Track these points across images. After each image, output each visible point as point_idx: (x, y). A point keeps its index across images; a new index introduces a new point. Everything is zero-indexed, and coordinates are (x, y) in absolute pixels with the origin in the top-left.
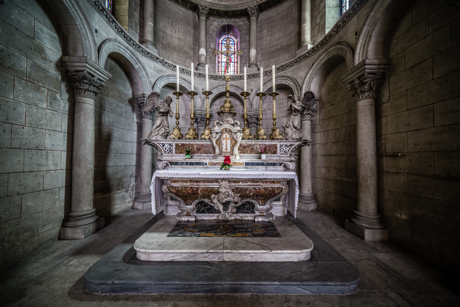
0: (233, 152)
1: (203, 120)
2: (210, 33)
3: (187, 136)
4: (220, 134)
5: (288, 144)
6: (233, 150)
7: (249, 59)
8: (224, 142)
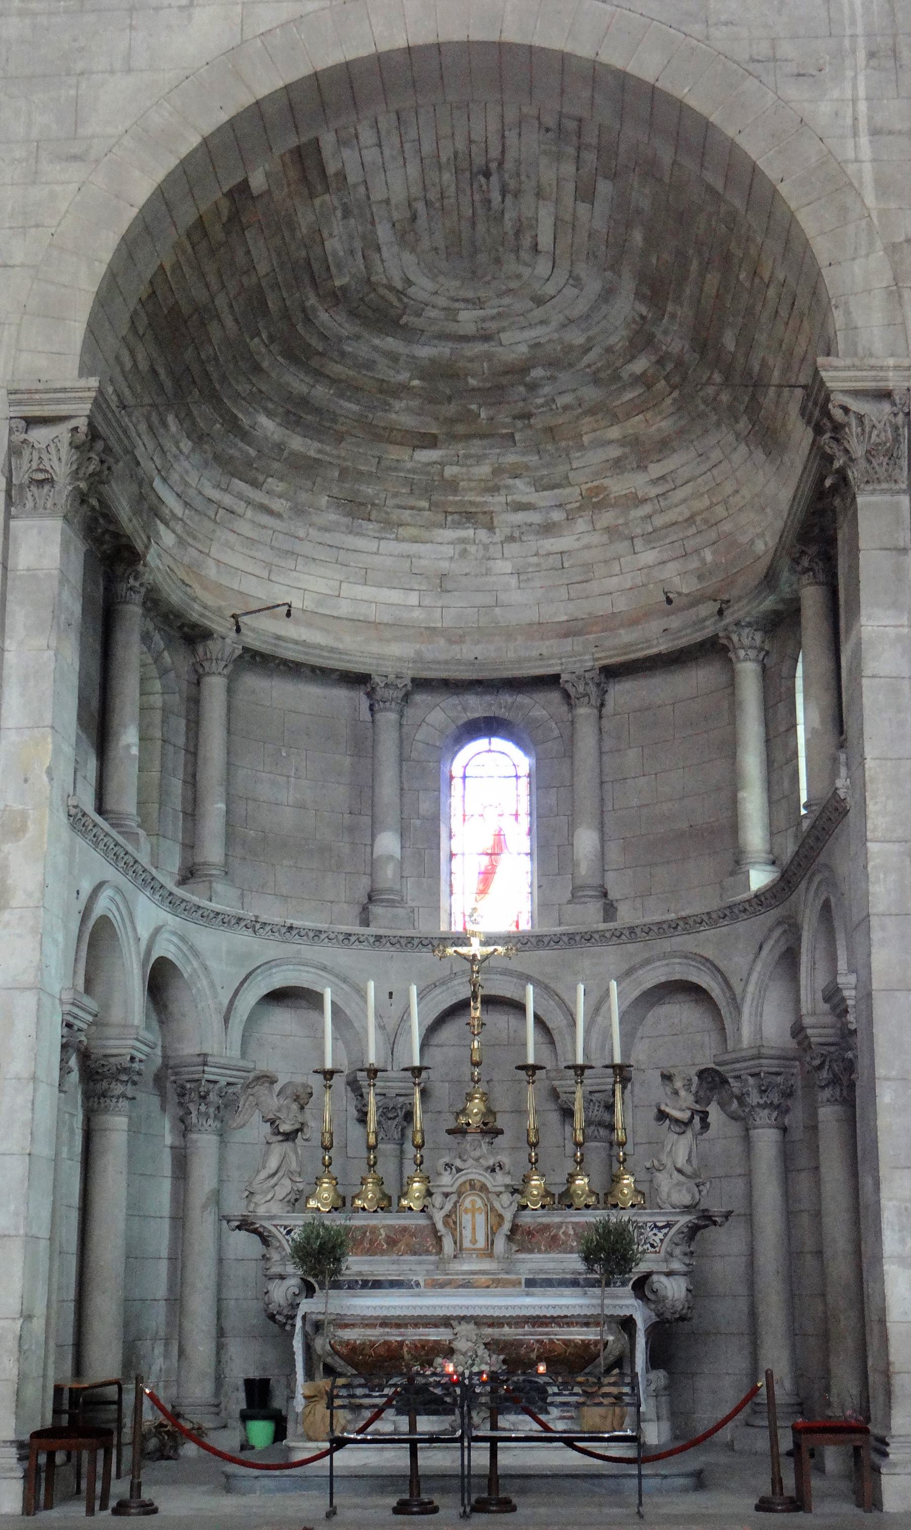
0: (492, 1249)
1: (391, 1115)
2: (414, 755)
3: (359, 1203)
4: (454, 1198)
5: (661, 1221)
6: (492, 1244)
7: (575, 864)
8: (466, 1219)
